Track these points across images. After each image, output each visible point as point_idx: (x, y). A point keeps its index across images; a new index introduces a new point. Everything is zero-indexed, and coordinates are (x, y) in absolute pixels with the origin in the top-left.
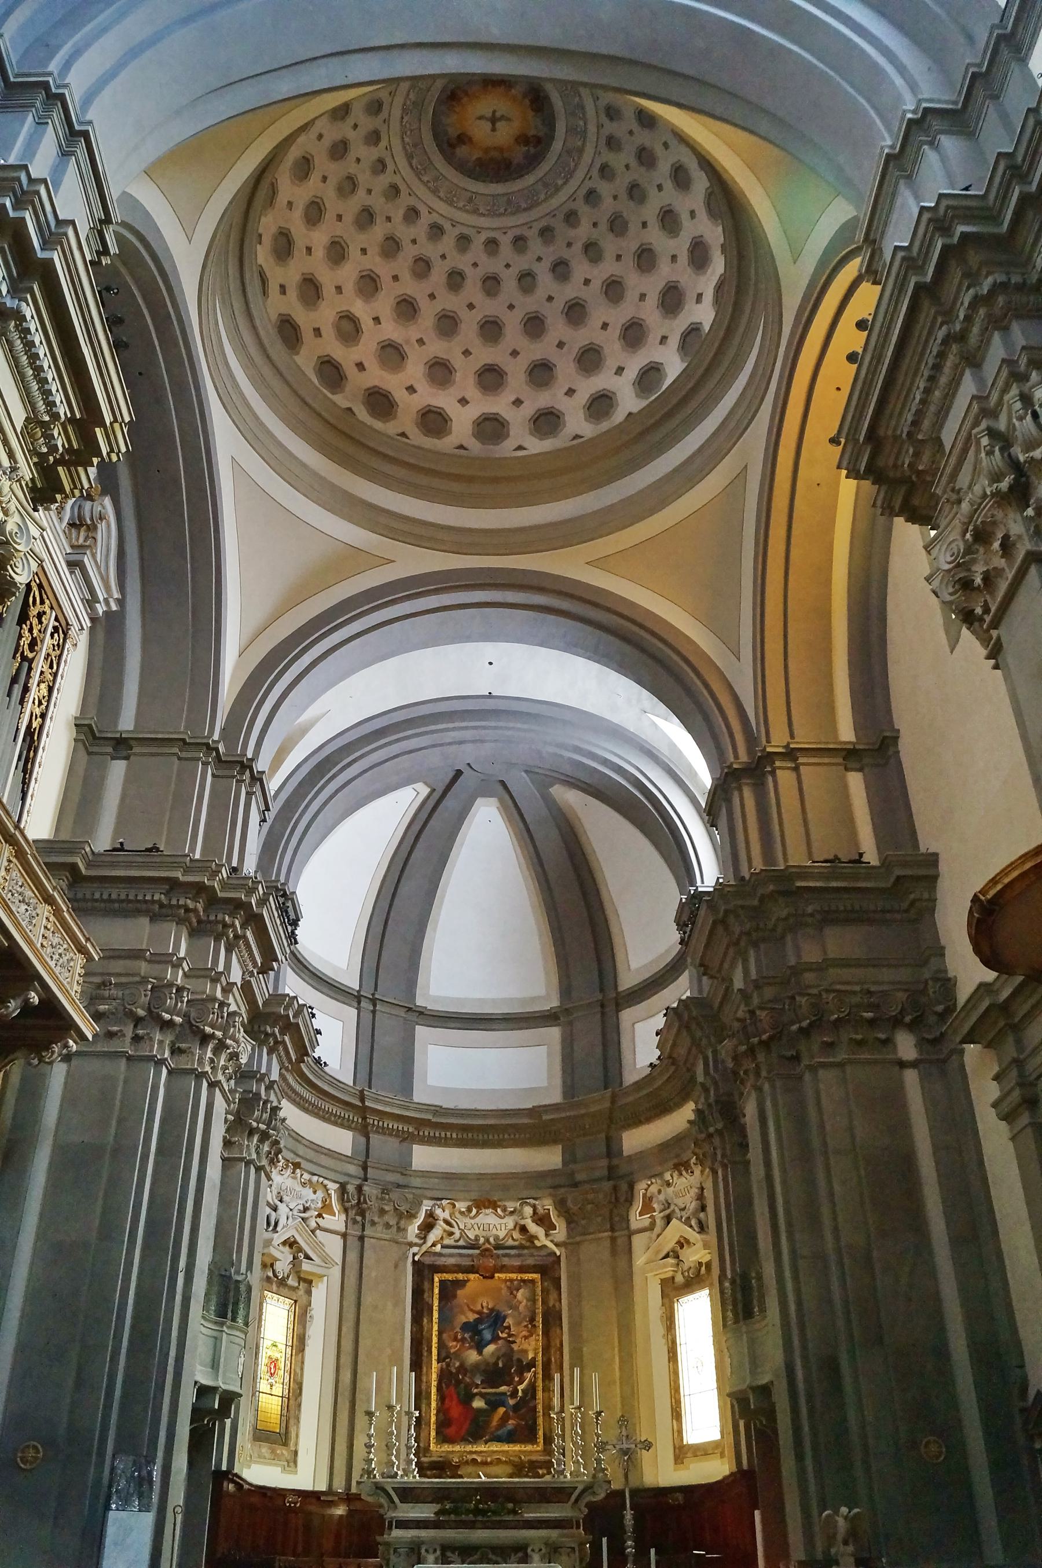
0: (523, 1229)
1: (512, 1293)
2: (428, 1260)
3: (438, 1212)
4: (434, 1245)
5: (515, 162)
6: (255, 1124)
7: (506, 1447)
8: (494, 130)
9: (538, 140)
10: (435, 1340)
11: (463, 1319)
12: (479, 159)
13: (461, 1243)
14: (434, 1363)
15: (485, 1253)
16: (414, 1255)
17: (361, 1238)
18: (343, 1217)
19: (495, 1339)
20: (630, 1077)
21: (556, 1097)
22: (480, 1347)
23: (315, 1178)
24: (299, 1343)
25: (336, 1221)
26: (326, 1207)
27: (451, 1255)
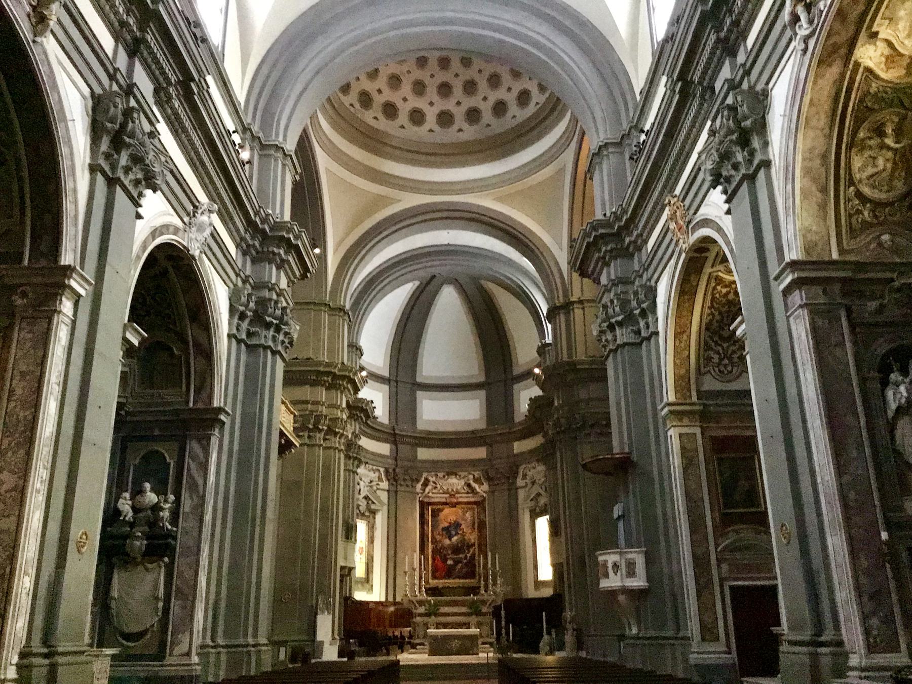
0: (469, 485)
2: (426, 500)
3: (430, 478)
6: (351, 454)
7: (462, 581)
10: (430, 535)
13: (441, 491)
14: (430, 544)
15: (452, 496)
17: (396, 492)
18: (387, 483)
19: (457, 534)
20: (517, 420)
21: (482, 425)
22: (450, 538)
23: (374, 467)
24: (371, 540)
25: (385, 485)
26: (380, 479)
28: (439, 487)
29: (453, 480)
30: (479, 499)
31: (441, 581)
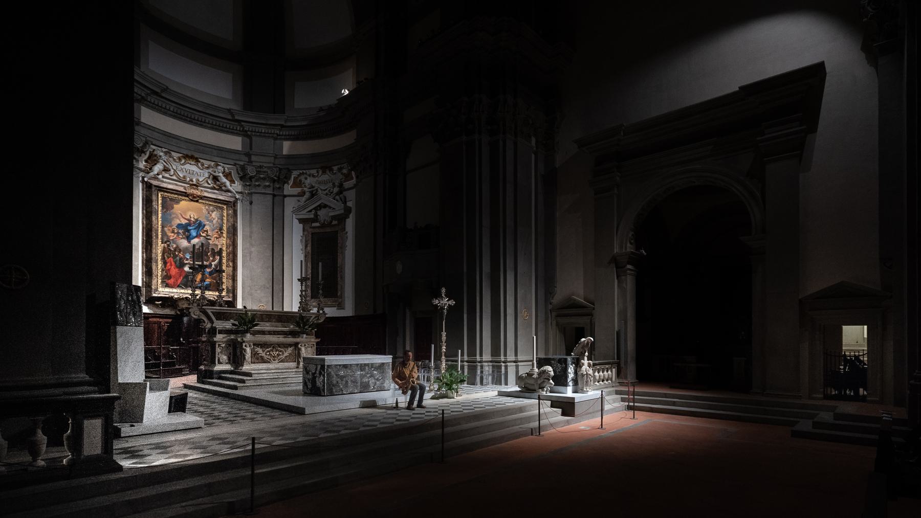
0: (215, 179)
1: (209, 213)
2: (154, 183)
4: (158, 174)
10: (160, 230)
11: (178, 222)
13: (174, 178)
14: (160, 243)
16: (143, 178)
19: (198, 236)
22: (189, 238)
27: (169, 183)
28: (172, 172)
29: (192, 167)
30: (232, 200)
31: (175, 290)
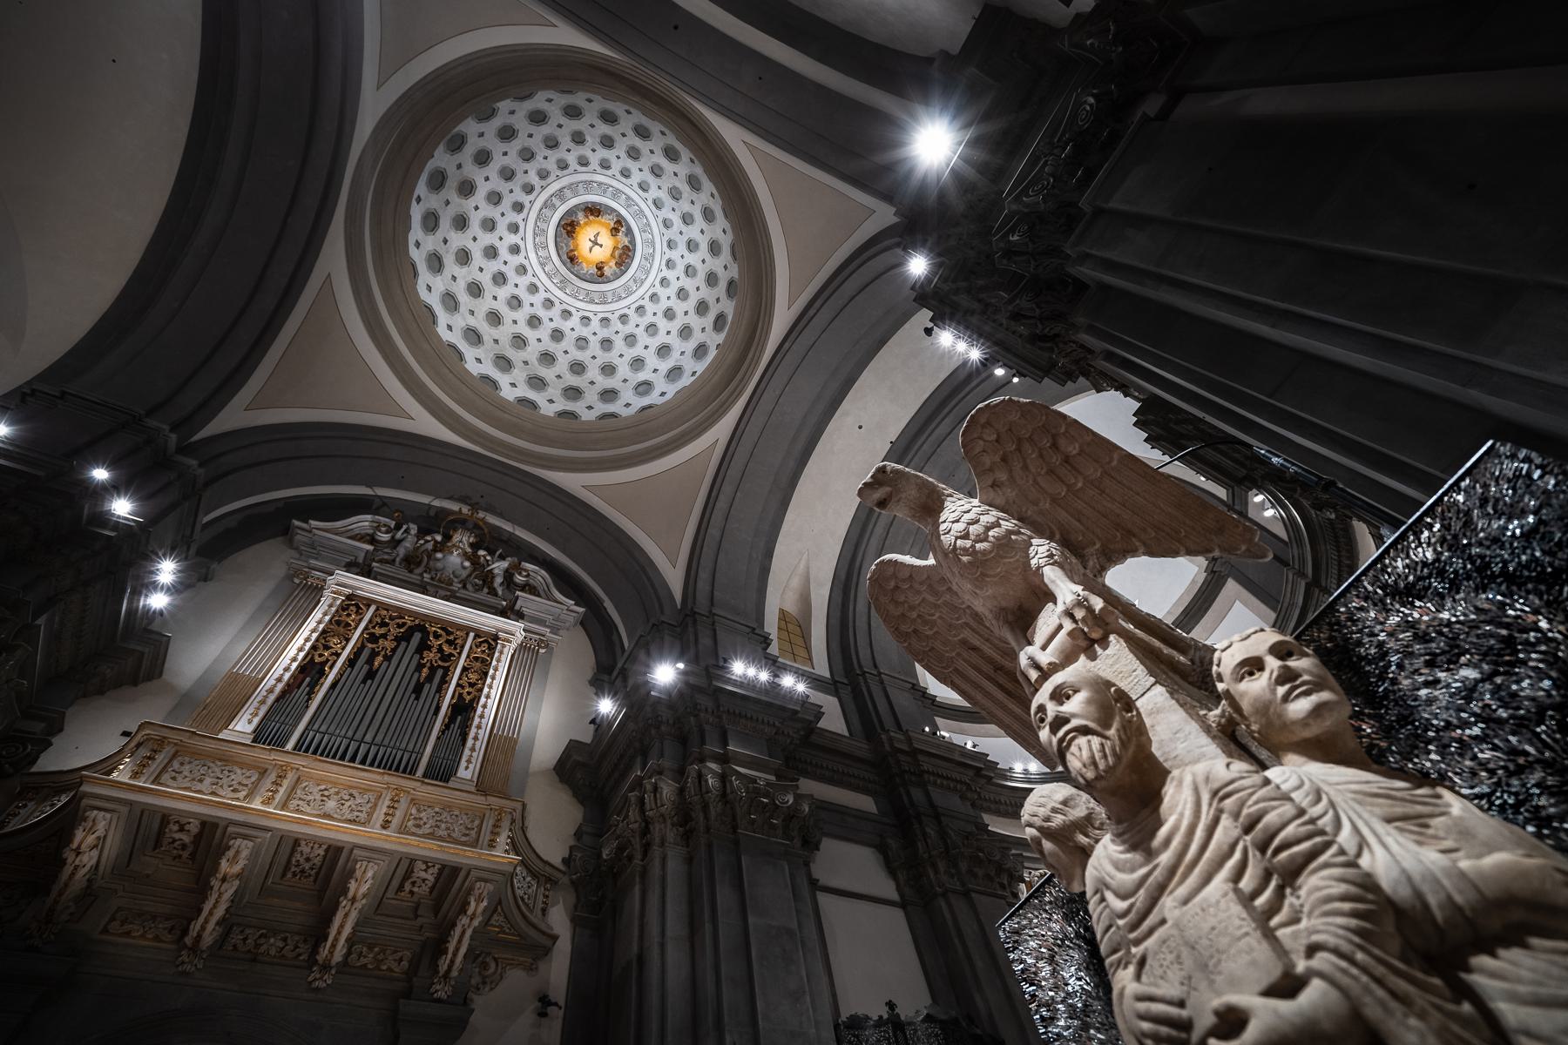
5: (627, 243)
8: (601, 246)
9: (619, 222)
12: (616, 263)
